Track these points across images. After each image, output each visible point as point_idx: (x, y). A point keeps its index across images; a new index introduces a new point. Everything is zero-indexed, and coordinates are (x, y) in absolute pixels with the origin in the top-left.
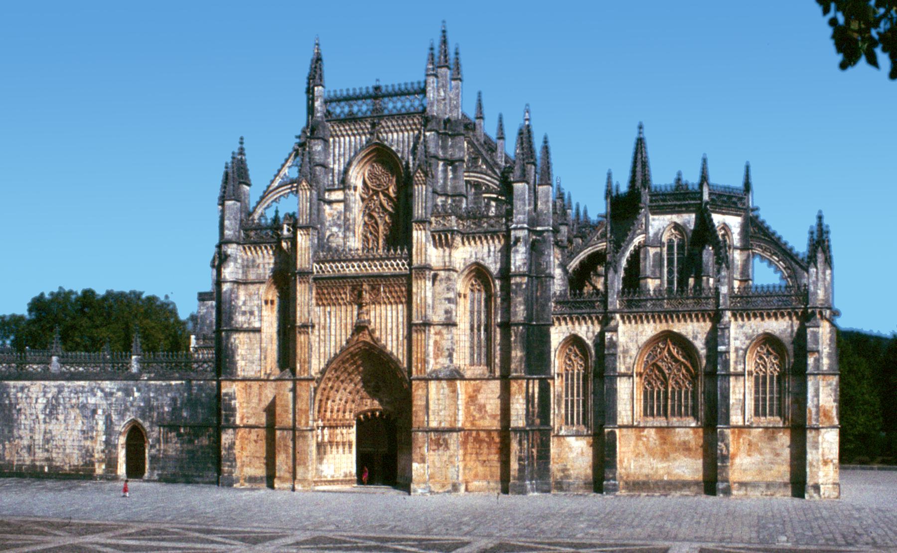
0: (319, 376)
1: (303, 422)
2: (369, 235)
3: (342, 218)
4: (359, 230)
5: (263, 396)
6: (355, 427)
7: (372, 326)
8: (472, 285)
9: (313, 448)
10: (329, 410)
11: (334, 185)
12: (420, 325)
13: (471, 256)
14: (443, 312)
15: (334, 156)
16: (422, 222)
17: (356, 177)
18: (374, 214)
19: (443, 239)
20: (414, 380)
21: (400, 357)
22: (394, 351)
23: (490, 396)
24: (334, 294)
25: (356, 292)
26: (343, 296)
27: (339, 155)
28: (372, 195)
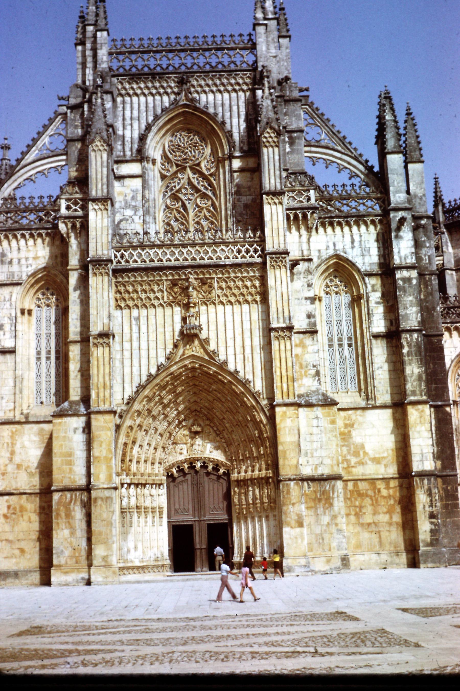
0: (124, 408)
1: (102, 477)
2: (172, 222)
3: (140, 197)
5: (18, 445)
6: (165, 485)
7: (203, 335)
8: (327, 286)
9: (117, 516)
10: (135, 461)
11: (124, 155)
12: (283, 329)
14: (304, 316)
15: (124, 119)
16: (276, 193)
17: (154, 149)
18: (180, 195)
19: (297, 218)
20: (279, 405)
21: (249, 377)
25: (176, 289)
26: (159, 295)
27: (131, 119)
28: (176, 173)
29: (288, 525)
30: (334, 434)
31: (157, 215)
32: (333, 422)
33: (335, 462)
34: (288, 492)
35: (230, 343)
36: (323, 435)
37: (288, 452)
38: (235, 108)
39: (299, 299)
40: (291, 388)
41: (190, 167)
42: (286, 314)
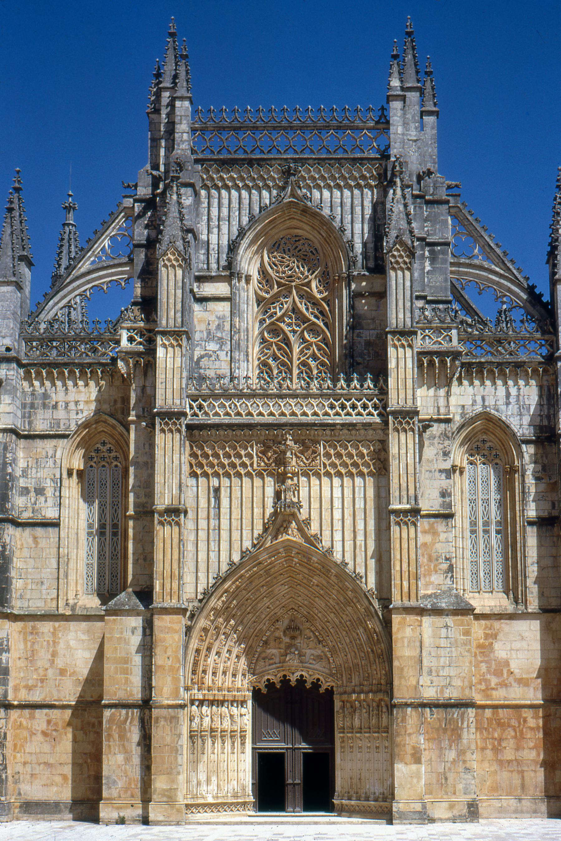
3: (227, 327)
4: (255, 350)
5: (62, 645)
7: (303, 514)
9: (184, 740)
13: (474, 401)
16: (406, 333)
21: (361, 570)
22: (348, 558)
23: (517, 645)
24: (228, 456)
29: (402, 760)
30: (467, 648)
31: (250, 350)
32: (467, 633)
33: (466, 683)
34: (404, 720)
35: (338, 526)
36: (453, 649)
37: (406, 670)
38: (358, 209)
39: (431, 471)
40: (413, 588)
41: (296, 287)
42: (412, 492)
